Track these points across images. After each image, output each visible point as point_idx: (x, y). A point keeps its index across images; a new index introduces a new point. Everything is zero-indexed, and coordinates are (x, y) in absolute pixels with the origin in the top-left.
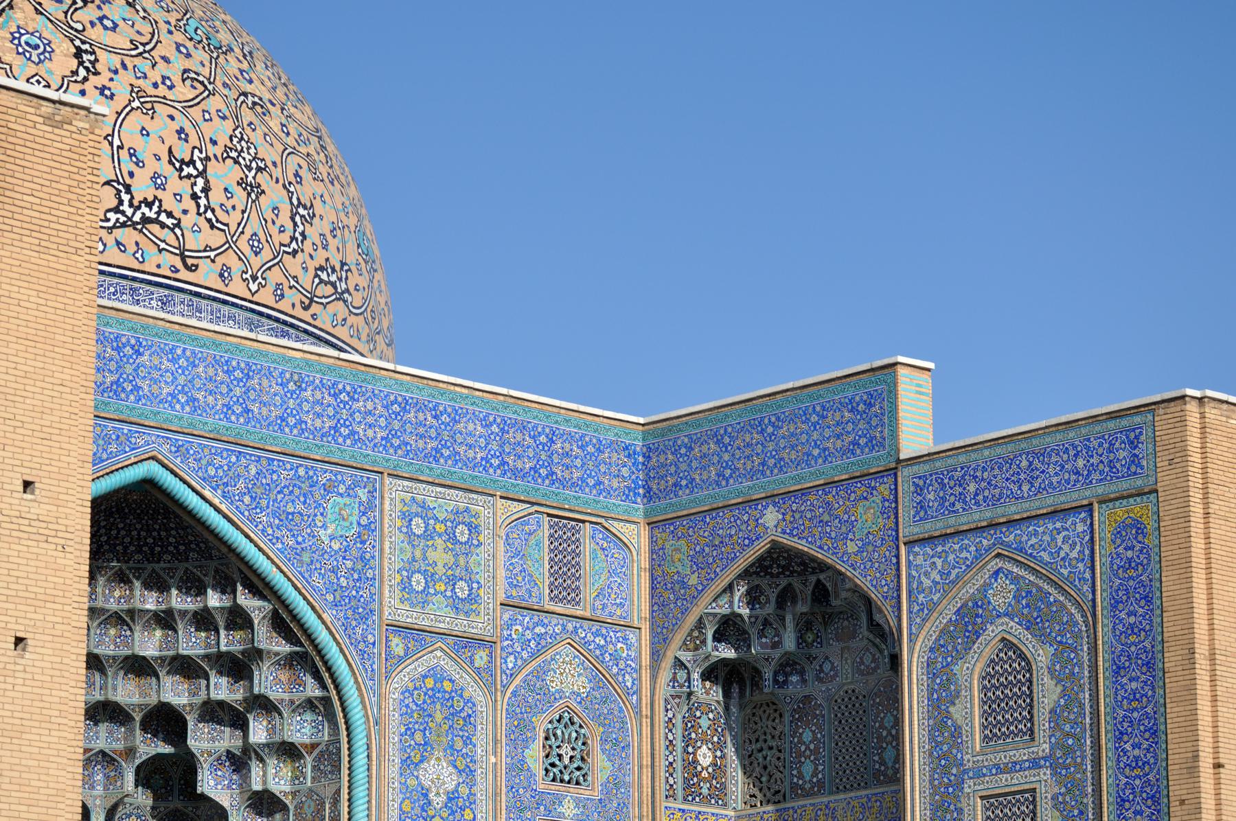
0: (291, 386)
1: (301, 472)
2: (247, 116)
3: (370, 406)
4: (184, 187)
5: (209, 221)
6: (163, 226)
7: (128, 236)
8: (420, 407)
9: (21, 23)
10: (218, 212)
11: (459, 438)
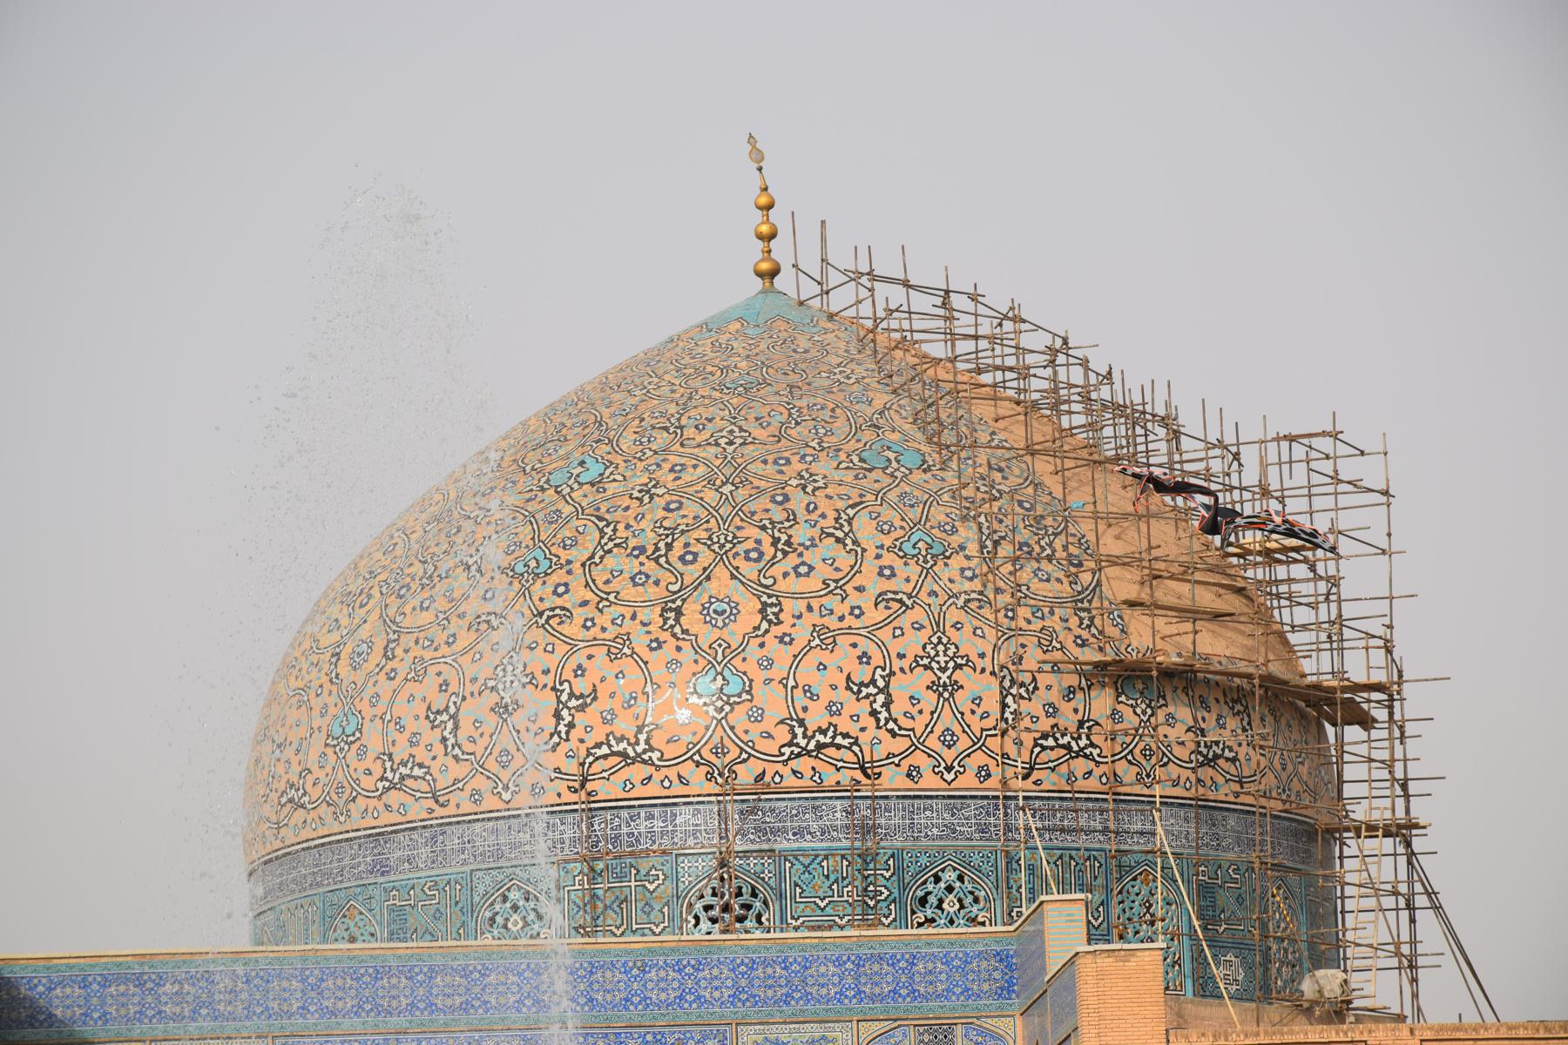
0: (635, 972)
1: (649, 1038)
2: (954, 615)
3: (715, 972)
4: (864, 708)
5: (891, 731)
6: (839, 747)
7: (803, 764)
8: (765, 963)
9: (713, 593)
10: (904, 722)
11: (810, 981)
